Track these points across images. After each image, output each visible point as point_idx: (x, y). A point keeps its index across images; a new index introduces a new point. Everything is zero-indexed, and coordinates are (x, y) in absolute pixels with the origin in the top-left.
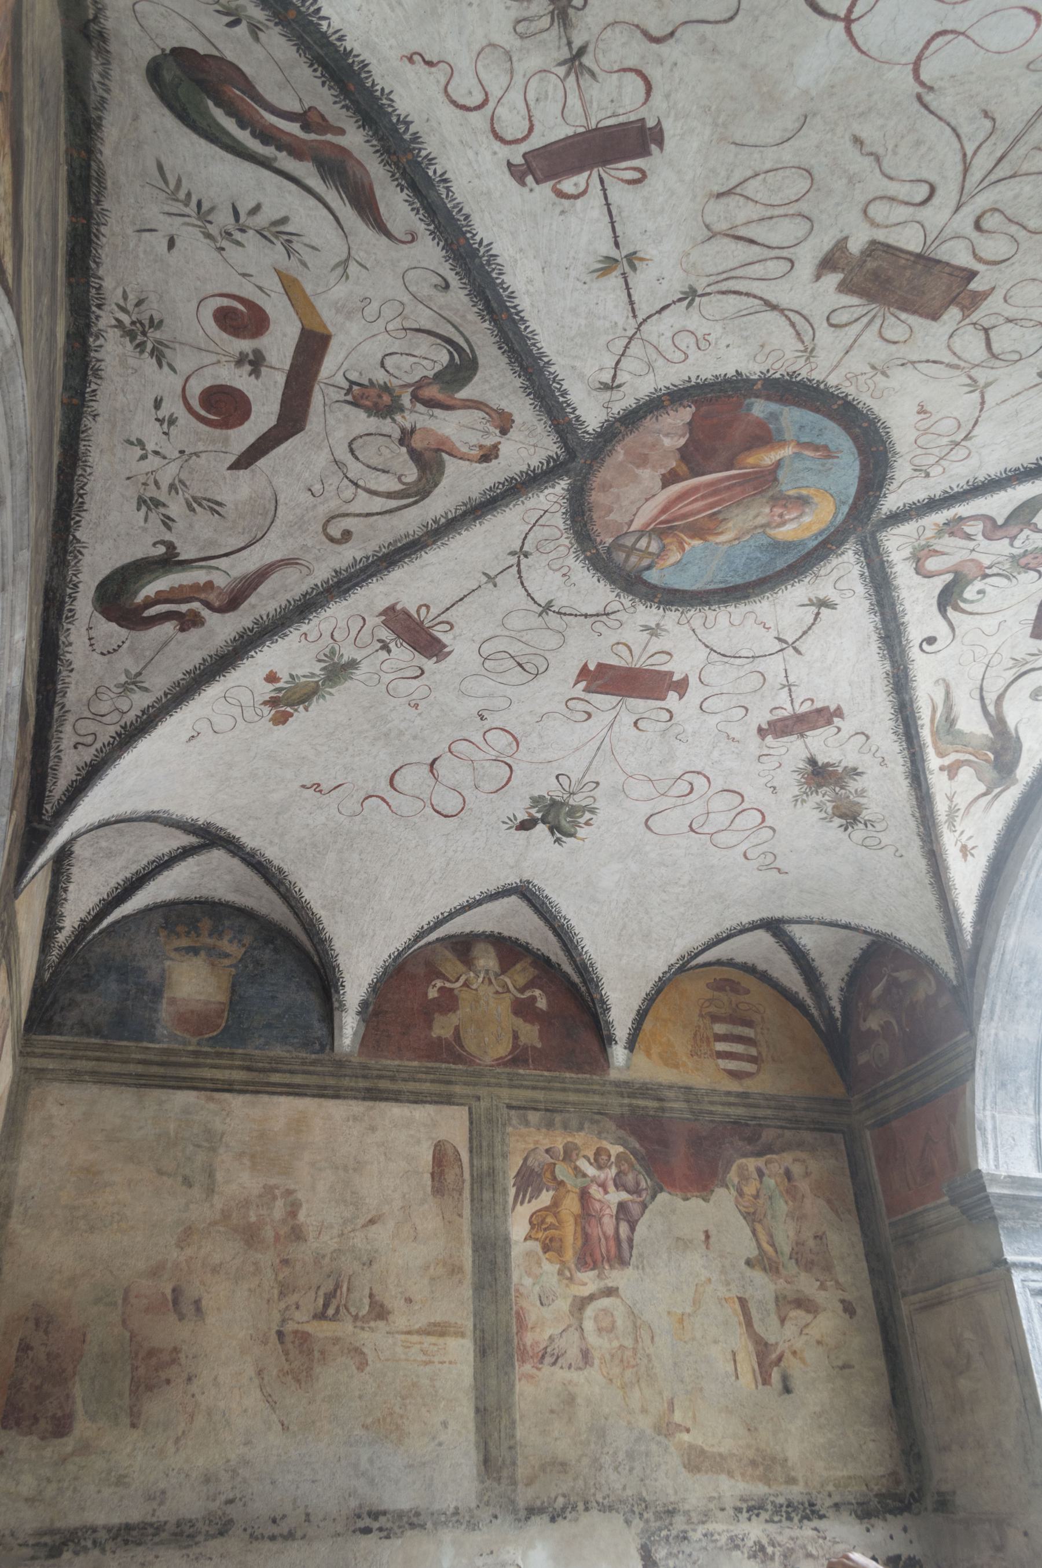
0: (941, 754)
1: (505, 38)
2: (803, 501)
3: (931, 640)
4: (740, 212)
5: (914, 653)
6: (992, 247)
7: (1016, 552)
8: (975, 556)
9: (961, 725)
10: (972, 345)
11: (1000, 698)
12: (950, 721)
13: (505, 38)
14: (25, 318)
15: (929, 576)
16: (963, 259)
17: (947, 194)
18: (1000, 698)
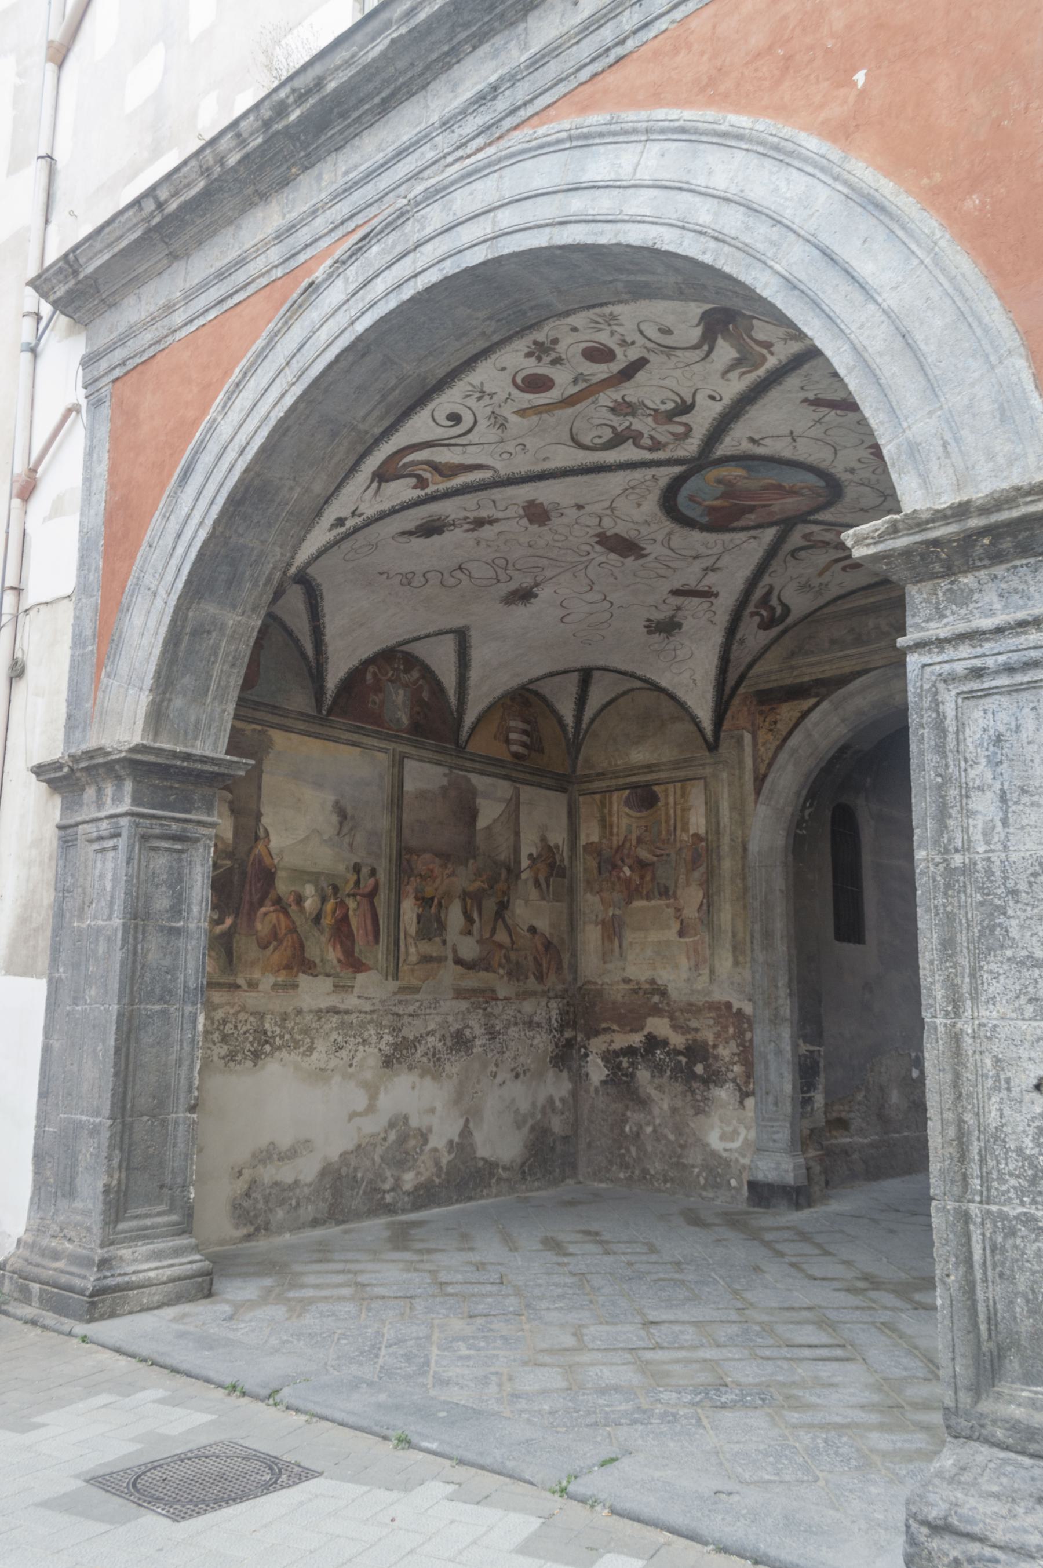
0: (764, 359)
1: (690, 618)
2: (719, 481)
3: (712, 398)
4: (663, 572)
5: (727, 401)
6: (588, 548)
7: (630, 418)
8: (654, 425)
9: (734, 354)
10: (607, 522)
11: (695, 348)
12: (737, 363)
13: (690, 618)
14: (847, 667)
15: (686, 425)
16: (598, 548)
17: (595, 563)
18: (695, 348)
